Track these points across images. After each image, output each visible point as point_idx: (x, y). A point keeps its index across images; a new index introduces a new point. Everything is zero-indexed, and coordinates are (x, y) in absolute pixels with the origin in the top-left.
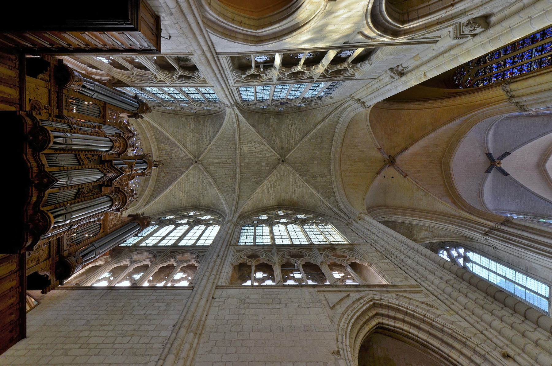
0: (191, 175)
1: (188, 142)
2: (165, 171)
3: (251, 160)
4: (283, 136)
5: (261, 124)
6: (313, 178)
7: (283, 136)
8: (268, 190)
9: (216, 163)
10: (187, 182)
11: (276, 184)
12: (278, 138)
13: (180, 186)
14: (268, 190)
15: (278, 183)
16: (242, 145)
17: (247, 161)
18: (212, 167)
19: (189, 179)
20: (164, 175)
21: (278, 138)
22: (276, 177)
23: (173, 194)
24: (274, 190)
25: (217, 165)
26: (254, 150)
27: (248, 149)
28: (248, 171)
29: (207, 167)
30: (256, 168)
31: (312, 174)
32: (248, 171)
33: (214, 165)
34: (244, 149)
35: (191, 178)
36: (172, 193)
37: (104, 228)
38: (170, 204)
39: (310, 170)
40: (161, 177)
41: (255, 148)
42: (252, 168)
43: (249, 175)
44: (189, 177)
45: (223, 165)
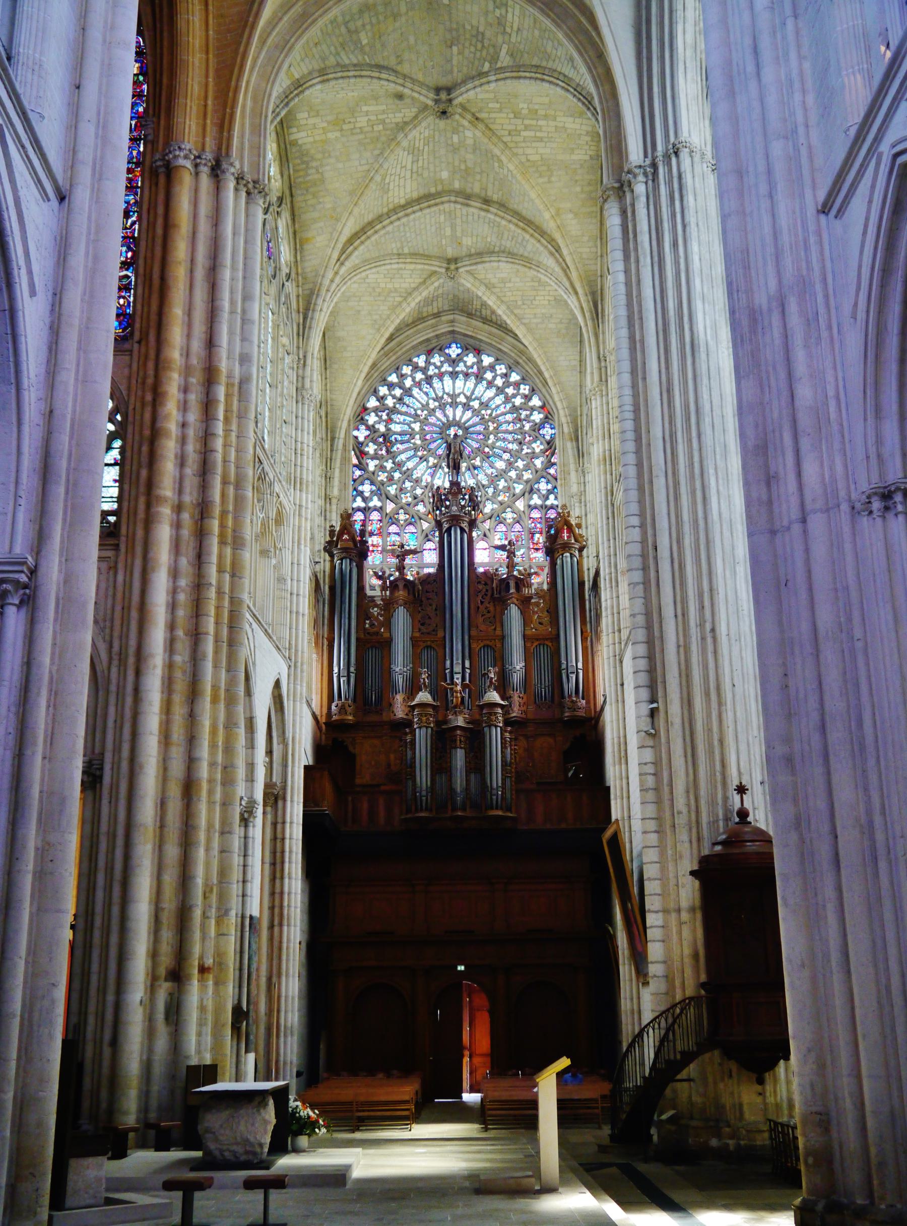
0: (490, 276)
1: (397, 286)
2: (478, 307)
3: (443, 165)
4: (355, 94)
5: (323, 181)
6: (508, 30)
7: (355, 94)
8: (541, 140)
9: (453, 227)
10: (508, 285)
11: (525, 112)
12: (365, 108)
13: (520, 303)
14: (541, 140)
15: (521, 106)
16: (396, 201)
17: (445, 175)
18: (467, 241)
19: (503, 281)
20: (489, 313)
21: (365, 108)
22: (500, 110)
23: (539, 320)
24: (546, 117)
25: (459, 229)
26: (409, 167)
27: (409, 181)
28: (478, 177)
29: (465, 249)
30: (469, 156)
31: (491, 25)
32: (478, 177)
33: (459, 234)
34: (408, 190)
35: (497, 276)
36: (537, 324)
37: (547, 639)
38: (564, 331)
39: (475, 22)
40: (494, 317)
41: (405, 167)
42: (470, 164)
43: (491, 176)
44: (494, 281)
45: (458, 221)
